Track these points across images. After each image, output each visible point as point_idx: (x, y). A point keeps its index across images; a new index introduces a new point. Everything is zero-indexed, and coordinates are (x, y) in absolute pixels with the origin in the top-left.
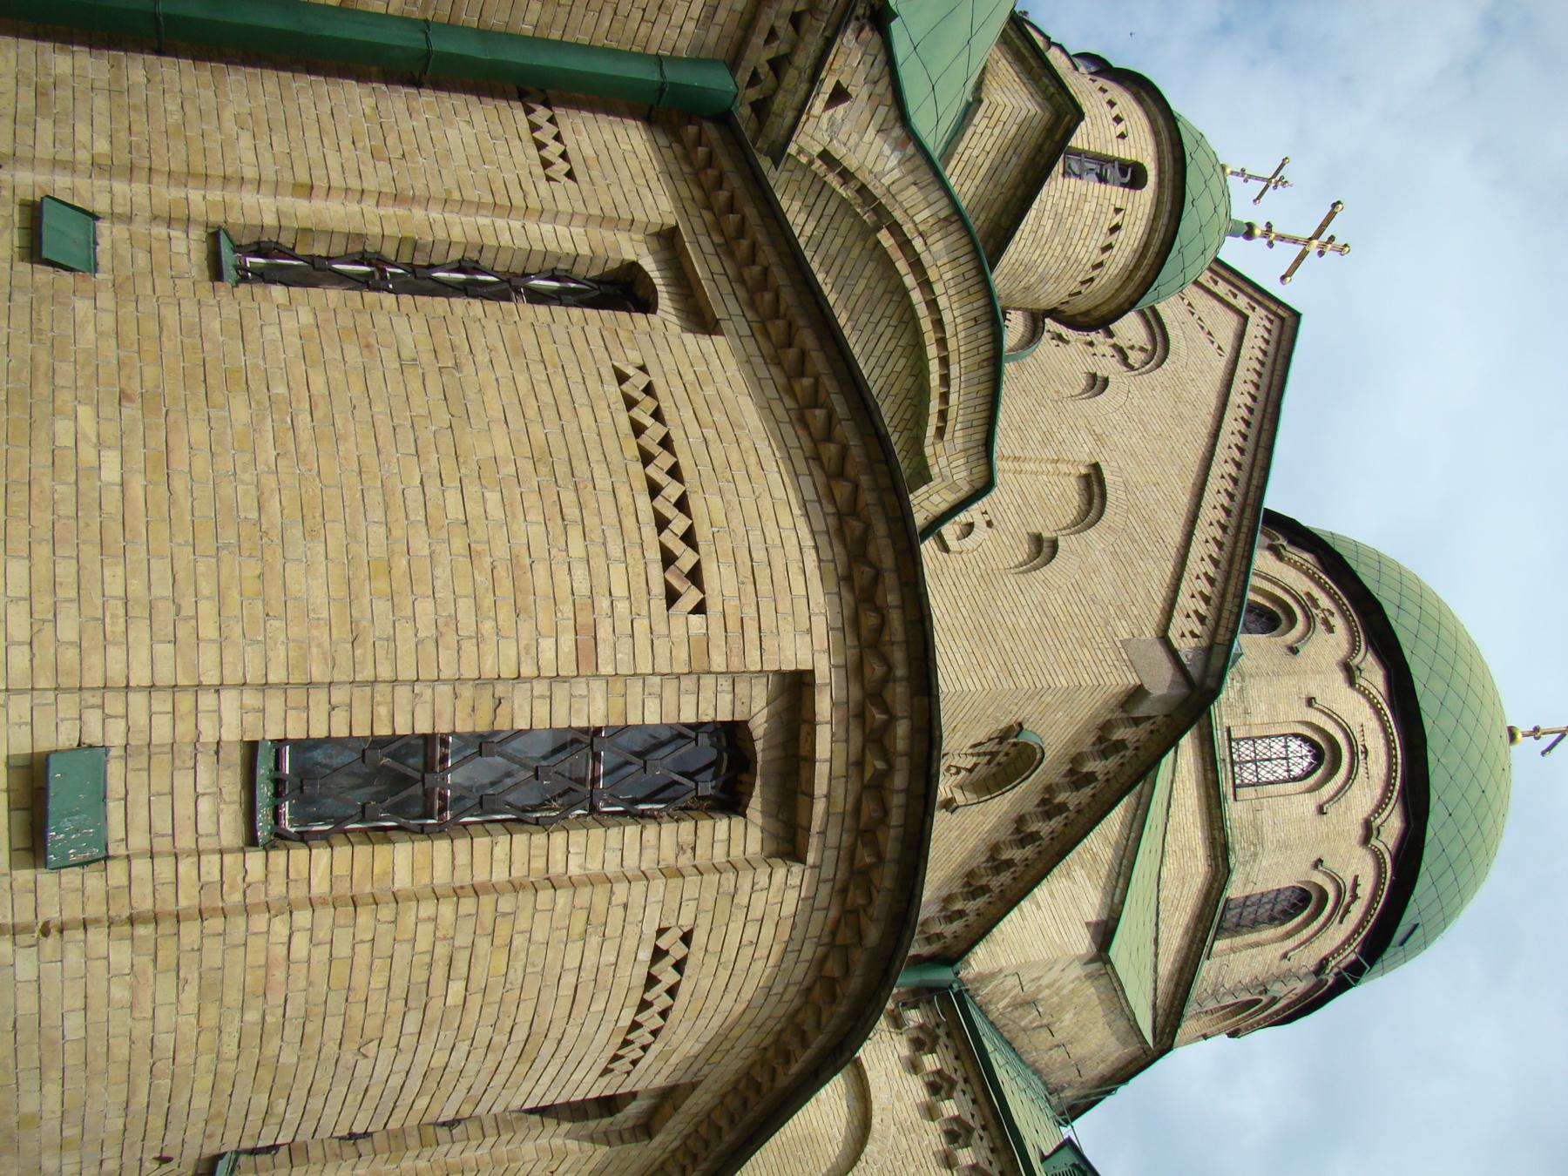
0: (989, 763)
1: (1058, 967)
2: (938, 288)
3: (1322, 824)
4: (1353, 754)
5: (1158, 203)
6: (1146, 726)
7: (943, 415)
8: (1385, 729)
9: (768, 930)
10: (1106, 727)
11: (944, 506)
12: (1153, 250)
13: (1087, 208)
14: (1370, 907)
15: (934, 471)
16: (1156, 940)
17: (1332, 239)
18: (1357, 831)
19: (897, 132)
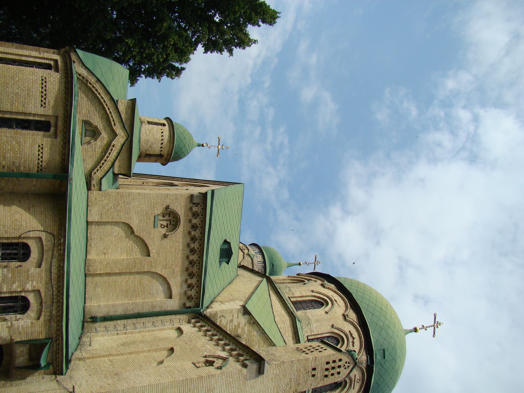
0: (170, 224)
1: (235, 315)
2: (101, 94)
3: (328, 316)
4: (331, 301)
5: (170, 128)
6: (199, 206)
7: (113, 121)
8: (340, 296)
9: (56, 80)
10: (191, 209)
11: (123, 142)
12: (172, 136)
13: (155, 129)
14: (361, 341)
15: (117, 133)
16: (284, 341)
17: (223, 145)
18: (342, 318)
19: (84, 67)
